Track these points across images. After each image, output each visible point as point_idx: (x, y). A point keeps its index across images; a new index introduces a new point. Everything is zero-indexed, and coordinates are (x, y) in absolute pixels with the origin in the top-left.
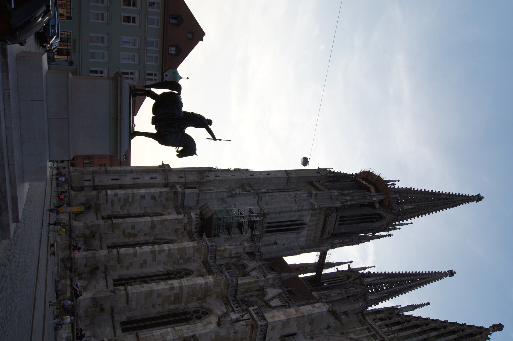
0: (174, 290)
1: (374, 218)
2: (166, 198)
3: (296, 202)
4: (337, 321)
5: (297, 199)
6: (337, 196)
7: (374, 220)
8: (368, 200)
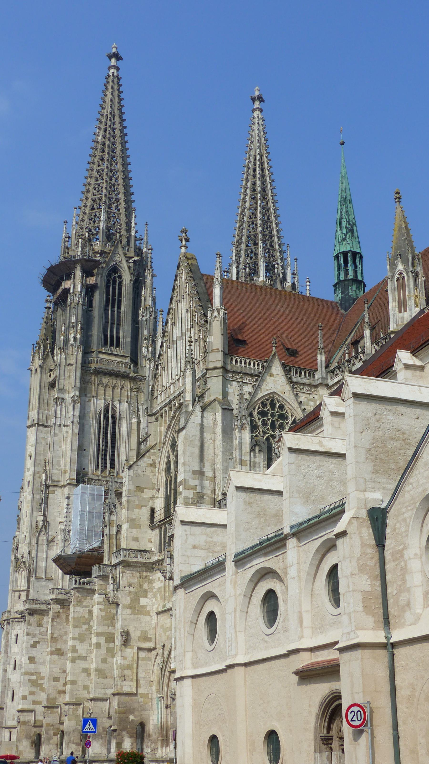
0: (100, 643)
1: (114, 282)
2: (37, 626)
3: (67, 426)
4: (148, 454)
5: (64, 422)
6: (67, 355)
7: (117, 283)
8: (80, 300)
